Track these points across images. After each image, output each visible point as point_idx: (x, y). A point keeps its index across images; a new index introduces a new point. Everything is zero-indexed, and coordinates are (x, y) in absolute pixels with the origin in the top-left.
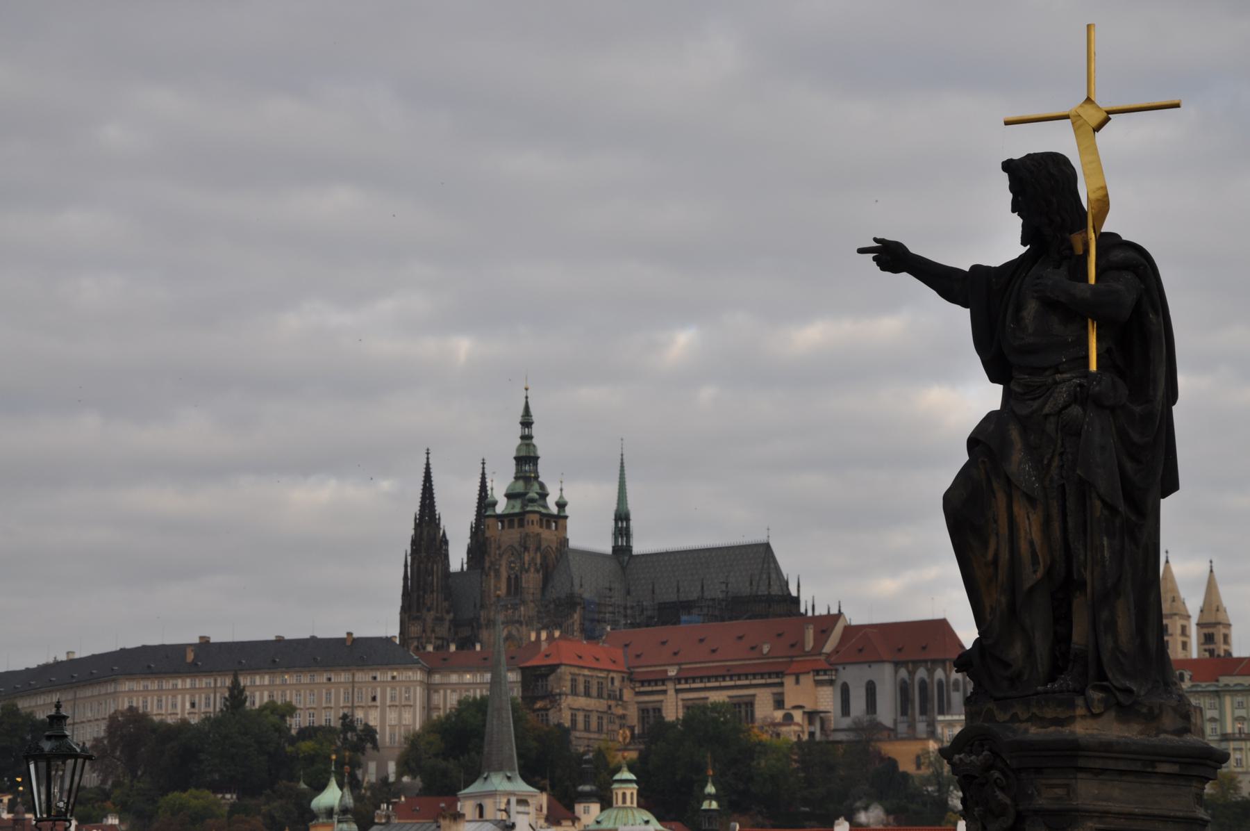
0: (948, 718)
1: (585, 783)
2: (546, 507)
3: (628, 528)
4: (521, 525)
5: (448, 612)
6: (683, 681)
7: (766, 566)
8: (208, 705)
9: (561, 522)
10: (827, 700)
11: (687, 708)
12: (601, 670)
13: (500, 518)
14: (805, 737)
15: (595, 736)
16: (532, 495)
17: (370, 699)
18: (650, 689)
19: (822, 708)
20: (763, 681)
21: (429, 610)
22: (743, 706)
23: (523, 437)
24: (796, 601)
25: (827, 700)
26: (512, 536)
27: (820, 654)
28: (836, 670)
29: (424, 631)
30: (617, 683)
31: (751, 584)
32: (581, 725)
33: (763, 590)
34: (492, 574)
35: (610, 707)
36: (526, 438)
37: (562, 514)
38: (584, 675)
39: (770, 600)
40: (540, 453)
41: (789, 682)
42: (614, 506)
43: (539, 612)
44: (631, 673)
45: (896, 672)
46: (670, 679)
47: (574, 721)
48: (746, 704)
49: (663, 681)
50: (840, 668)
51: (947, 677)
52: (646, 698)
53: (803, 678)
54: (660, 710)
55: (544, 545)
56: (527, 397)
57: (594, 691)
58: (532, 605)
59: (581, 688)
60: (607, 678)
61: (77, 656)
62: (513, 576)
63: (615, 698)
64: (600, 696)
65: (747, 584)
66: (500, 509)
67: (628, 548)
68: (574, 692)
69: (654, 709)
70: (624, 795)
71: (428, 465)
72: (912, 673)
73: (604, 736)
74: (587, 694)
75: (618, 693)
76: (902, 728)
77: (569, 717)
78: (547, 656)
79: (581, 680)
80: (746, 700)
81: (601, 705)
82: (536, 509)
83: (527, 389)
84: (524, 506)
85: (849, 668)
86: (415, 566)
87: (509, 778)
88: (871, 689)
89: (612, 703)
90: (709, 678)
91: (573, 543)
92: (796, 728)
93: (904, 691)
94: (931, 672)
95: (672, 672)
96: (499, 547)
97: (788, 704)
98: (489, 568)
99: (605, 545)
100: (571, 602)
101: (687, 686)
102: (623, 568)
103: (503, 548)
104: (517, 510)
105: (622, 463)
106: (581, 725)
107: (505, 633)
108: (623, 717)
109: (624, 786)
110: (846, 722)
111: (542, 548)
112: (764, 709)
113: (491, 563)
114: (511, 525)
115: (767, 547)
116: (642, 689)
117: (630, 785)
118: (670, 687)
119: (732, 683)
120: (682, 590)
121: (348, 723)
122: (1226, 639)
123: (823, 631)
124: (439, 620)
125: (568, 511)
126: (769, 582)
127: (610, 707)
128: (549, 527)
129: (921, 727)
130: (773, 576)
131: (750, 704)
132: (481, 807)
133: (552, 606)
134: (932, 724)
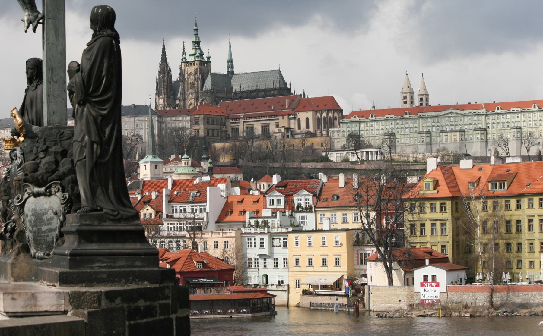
0: (332, 129)
2: (203, 58)
4: (194, 65)
5: (172, 95)
9: (208, 63)
11: (247, 128)
18: (235, 121)
19: (291, 127)
24: (289, 89)
26: (191, 69)
28: (296, 114)
30: (223, 120)
32: (211, 134)
35: (221, 128)
44: (228, 116)
46: (241, 118)
47: (208, 133)
48: (267, 126)
50: (297, 113)
52: (233, 125)
54: (238, 129)
55: (202, 72)
57: (215, 123)
59: (210, 122)
63: (223, 125)
64: (217, 124)
68: (208, 123)
69: (236, 128)
72: (321, 115)
73: (219, 138)
74: (213, 124)
79: (210, 119)
80: (267, 125)
81: (218, 127)
84: (195, 58)
87: (154, 157)
88: (307, 120)
89: (222, 126)
95: (242, 116)
97: (280, 126)
101: (247, 120)
103: (188, 73)
104: (193, 60)
106: (211, 134)
107: (189, 102)
108: (226, 131)
112: (273, 129)
115: (279, 70)
116: (232, 122)
118: (242, 121)
119: (262, 119)
122: (427, 99)
125: (211, 60)
127: (221, 128)
128: (204, 65)
129: (324, 132)
131: (268, 126)
132: (145, 166)
134: (327, 132)
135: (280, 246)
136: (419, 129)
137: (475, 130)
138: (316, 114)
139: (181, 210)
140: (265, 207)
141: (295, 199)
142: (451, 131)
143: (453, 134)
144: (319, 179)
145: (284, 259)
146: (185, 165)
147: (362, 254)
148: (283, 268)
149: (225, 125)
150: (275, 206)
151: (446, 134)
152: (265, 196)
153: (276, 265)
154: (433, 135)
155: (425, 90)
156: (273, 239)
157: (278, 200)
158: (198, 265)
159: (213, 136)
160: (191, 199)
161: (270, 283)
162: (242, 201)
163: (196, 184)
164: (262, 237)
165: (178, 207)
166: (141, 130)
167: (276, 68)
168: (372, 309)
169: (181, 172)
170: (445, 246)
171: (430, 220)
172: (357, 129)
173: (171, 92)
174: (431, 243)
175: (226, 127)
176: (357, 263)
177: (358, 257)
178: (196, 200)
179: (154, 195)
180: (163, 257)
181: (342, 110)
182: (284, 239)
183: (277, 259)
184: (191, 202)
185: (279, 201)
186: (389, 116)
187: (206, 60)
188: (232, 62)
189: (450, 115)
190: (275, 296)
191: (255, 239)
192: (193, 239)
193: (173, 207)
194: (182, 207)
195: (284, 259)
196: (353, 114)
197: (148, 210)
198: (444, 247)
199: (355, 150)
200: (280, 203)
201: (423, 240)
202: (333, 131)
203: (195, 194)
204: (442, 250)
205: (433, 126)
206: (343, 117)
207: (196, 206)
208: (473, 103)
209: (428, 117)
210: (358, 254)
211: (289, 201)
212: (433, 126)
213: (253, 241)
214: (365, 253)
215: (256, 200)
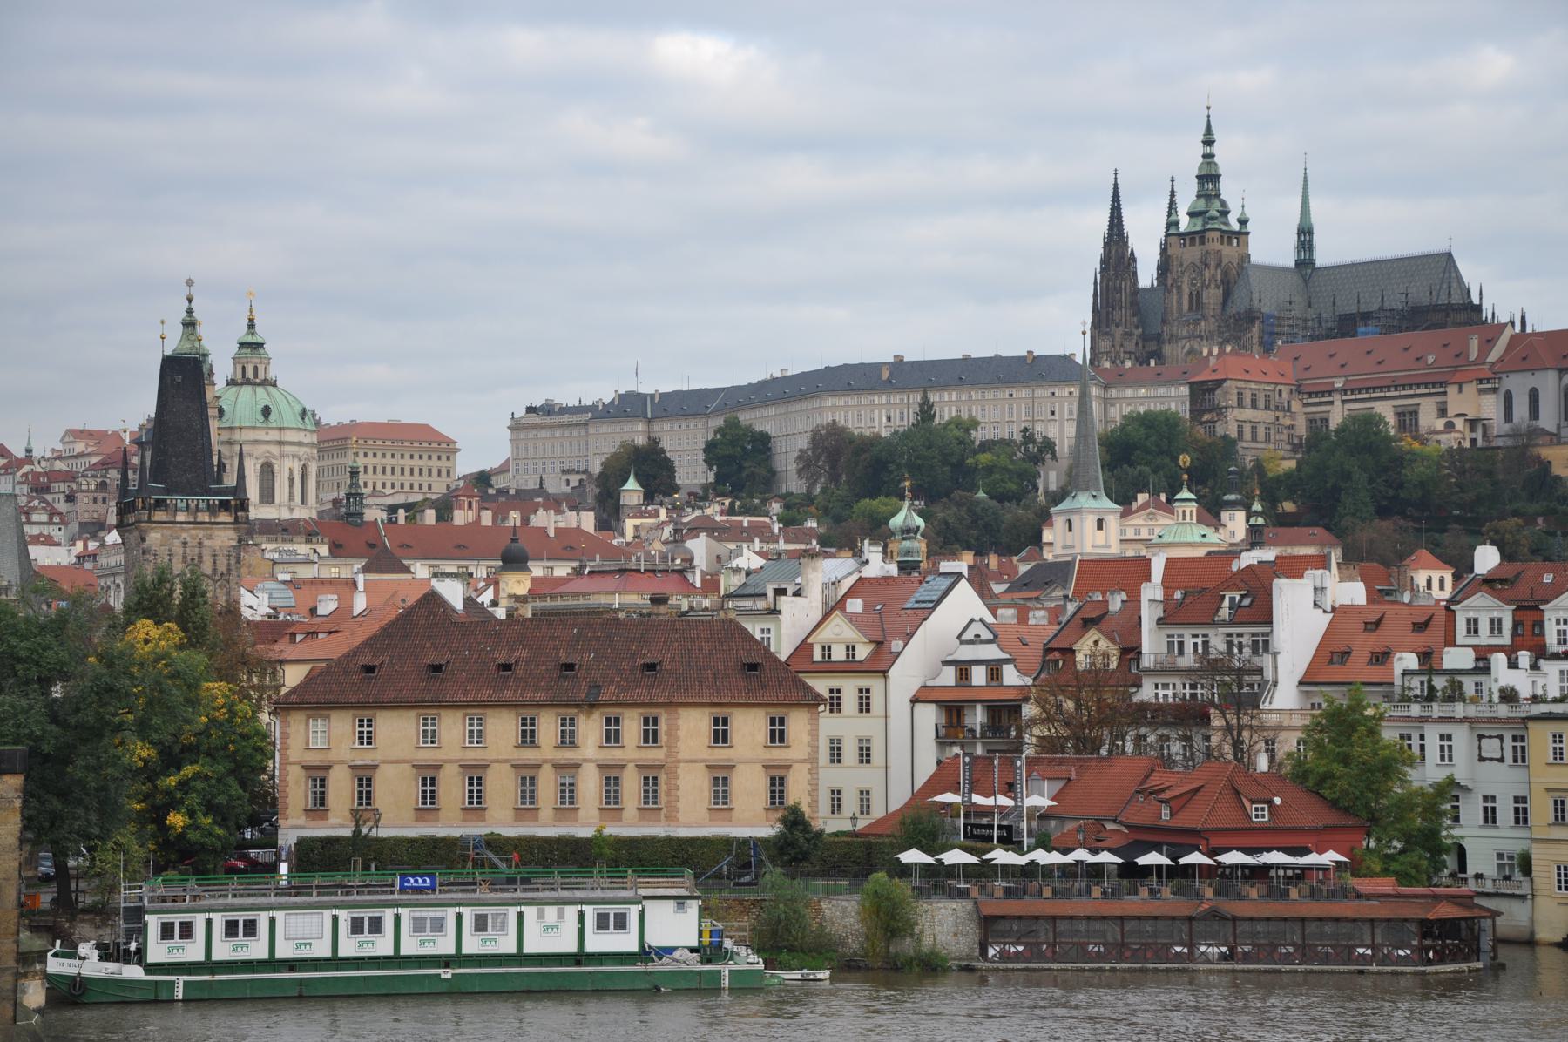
1: (1231, 493)
2: (1227, 224)
3: (1310, 242)
4: (1202, 242)
5: (1137, 327)
6: (1349, 393)
7: (1447, 275)
8: (902, 419)
9: (1242, 238)
10: (1490, 408)
12: (1269, 383)
13: (1182, 235)
14: (1467, 444)
15: (1263, 446)
16: (1213, 213)
17: (1049, 413)
18: (1317, 400)
19: (1484, 416)
20: (1427, 391)
21: (1117, 326)
22: (1408, 416)
23: (1204, 156)
24: (1478, 308)
25: (1490, 408)
26: (1192, 253)
27: (1484, 363)
28: (1500, 379)
29: (1113, 346)
30: (1285, 395)
31: (1431, 293)
32: (1247, 436)
33: (1443, 300)
34: (1175, 291)
35: (1277, 418)
36: (1208, 157)
37: (1243, 230)
38: (1251, 389)
39: (1449, 309)
40: (1221, 171)
41: (1452, 391)
42: (1297, 221)
43: (1219, 326)
45: (1560, 379)
46: (1336, 390)
47: (1241, 433)
48: (1411, 413)
49: (1330, 393)
50: (1504, 376)
52: (1314, 409)
53: (1465, 387)
54: (1327, 420)
55: (1225, 261)
56: (1209, 116)
57: (1261, 404)
58: (1213, 319)
59: (1248, 401)
60: (1274, 390)
61: (789, 373)
62: (1194, 293)
63: (1283, 410)
64: (1267, 408)
65: (1428, 294)
67: (1311, 262)
68: (1240, 405)
69: (1322, 420)
70: (1184, 511)
71: (1116, 185)
73: (1272, 446)
74: (1254, 406)
75: (1286, 405)
77: (1236, 429)
78: (1214, 371)
80: (1411, 409)
81: (1269, 416)
82: (1217, 226)
83: (1208, 108)
84: (1205, 223)
85: (1512, 376)
86: (1104, 285)
87: (1094, 497)
88: (1534, 396)
89: (1280, 414)
90: (1374, 389)
91: (1255, 259)
92: (1457, 435)
95: (1339, 384)
96: (1181, 265)
97: (1451, 412)
98: (1172, 285)
99: (1286, 257)
100: (1250, 317)
101: (1353, 397)
102: (1306, 281)
105: (1305, 178)
106: (1247, 436)
107: (1187, 348)
108: (1291, 427)
109: (1184, 504)
110: (1506, 427)
111: (1223, 264)
112: (1428, 418)
113: (1174, 280)
114: (1192, 243)
115: (1449, 256)
116: (1310, 401)
117: (1189, 504)
118: (1337, 398)
119: (1397, 393)
120: (1361, 302)
121: (1027, 435)
123: (1489, 341)
124: (1128, 335)
125: (1250, 227)
126: (1450, 292)
127: (1277, 418)
128: (1230, 243)
130: (1454, 285)
131: (1414, 414)
132: (1070, 522)
133: (1232, 320)
135: (1501, 760)
138: (1560, 379)
139: (1195, 645)
140: (1451, 643)
141: (1546, 618)
145: (1517, 800)
146: (1184, 519)
148: (1511, 827)
149: (1289, 410)
150: (1484, 638)
152: (1453, 607)
153: (1490, 817)
156: (1481, 737)
157: (1492, 621)
159: (1254, 439)
160: (1225, 612)
161: (1471, 870)
162: (1378, 623)
163: (1239, 571)
164: (1446, 729)
166: (1052, 423)
167: (1443, 248)
169: (1170, 540)
173: (1135, 319)
175: (1293, 416)
178: (1239, 616)
179: (1116, 602)
180: (1150, 783)
182: (1515, 739)
183: (1493, 798)
184: (1223, 623)
185: (1496, 625)
187: (1236, 227)
188: (1310, 232)
190: (1499, 914)
191: (1422, 737)
192: (1235, 733)
193: (1173, 636)
194: (1196, 636)
195: (1517, 800)
197: (1096, 643)
203: (1238, 598)
207: (1240, 635)
211: (1528, 623)
213: (1415, 742)
215: (1423, 620)
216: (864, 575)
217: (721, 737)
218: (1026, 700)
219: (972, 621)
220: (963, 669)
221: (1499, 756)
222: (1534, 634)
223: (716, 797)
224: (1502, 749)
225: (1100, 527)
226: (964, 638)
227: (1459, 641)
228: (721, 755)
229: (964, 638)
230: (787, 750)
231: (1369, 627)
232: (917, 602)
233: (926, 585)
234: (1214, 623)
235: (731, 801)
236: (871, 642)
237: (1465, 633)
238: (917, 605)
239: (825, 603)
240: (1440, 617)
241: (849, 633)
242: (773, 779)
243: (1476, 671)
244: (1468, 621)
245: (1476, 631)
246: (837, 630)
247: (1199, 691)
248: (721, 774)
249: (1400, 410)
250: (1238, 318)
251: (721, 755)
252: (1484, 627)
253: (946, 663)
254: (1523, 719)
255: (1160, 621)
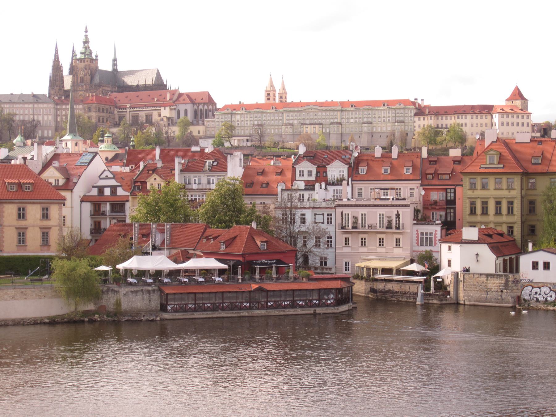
0: (208, 119)
2: (92, 57)
3: (116, 63)
4: (84, 62)
24: (166, 86)
30: (112, 109)
36: (86, 36)
51: (208, 108)
59: (101, 110)
63: (112, 113)
64: (107, 112)
66: (78, 57)
67: (116, 70)
68: (99, 111)
72: (198, 107)
74: (103, 112)
76: (195, 122)
81: (108, 115)
84: (85, 56)
87: (75, 135)
88: (186, 112)
89: (110, 115)
93: (196, 112)
94: (203, 106)
95: (128, 106)
97: (162, 116)
104: (83, 58)
107: (79, 94)
112: (155, 118)
114: (81, 62)
118: (128, 110)
122: (286, 98)
125: (98, 58)
128: (93, 62)
129: (200, 122)
131: (151, 115)
134: (203, 121)
135: (323, 223)
136: (283, 122)
137: (332, 123)
139: (195, 180)
142: (311, 124)
143: (312, 126)
144: (351, 149)
147: (422, 234)
150: (306, 178)
151: (307, 126)
152: (295, 166)
154: (295, 127)
155: (284, 89)
156: (315, 214)
157: (309, 171)
158: (262, 245)
160: (206, 168)
165: (193, 177)
168: (462, 300)
169: (104, 149)
170: (512, 227)
171: (494, 198)
172: (230, 119)
174: (494, 223)
176: (416, 243)
177: (418, 237)
178: (212, 170)
181: (216, 104)
182: (328, 215)
186: (258, 110)
187: (94, 58)
189: (310, 110)
194: (196, 177)
196: (226, 107)
197: (155, 179)
198: (511, 229)
199: (229, 138)
200: (311, 175)
201: (484, 219)
202: (208, 121)
203: (212, 162)
204: (509, 231)
205: (296, 119)
206: (217, 110)
208: (329, 100)
209: (291, 111)
210: (418, 234)
212: (296, 119)
214: (430, 233)
216: (56, 152)
217: (21, 215)
218: (128, 201)
219: (105, 170)
220: (101, 190)
221: (322, 221)
222: (323, 176)
223: (20, 241)
224: (323, 219)
225: (76, 145)
226: (101, 177)
227: (296, 179)
228: (22, 223)
229: (101, 177)
230: (49, 221)
231: (259, 174)
232: (81, 163)
233: (83, 157)
234: (203, 172)
235: (26, 242)
236: (65, 178)
237: (307, 176)
238: (81, 164)
239: (43, 163)
240: (289, 172)
241: (57, 175)
242: (43, 233)
243: (305, 190)
244: (300, 171)
245: (303, 175)
246: (52, 173)
247: (198, 198)
248: (21, 231)
249: (147, 114)
250: (96, 86)
251: (22, 223)
252: (306, 174)
253: (94, 187)
254: (335, 207)
255: (182, 171)
